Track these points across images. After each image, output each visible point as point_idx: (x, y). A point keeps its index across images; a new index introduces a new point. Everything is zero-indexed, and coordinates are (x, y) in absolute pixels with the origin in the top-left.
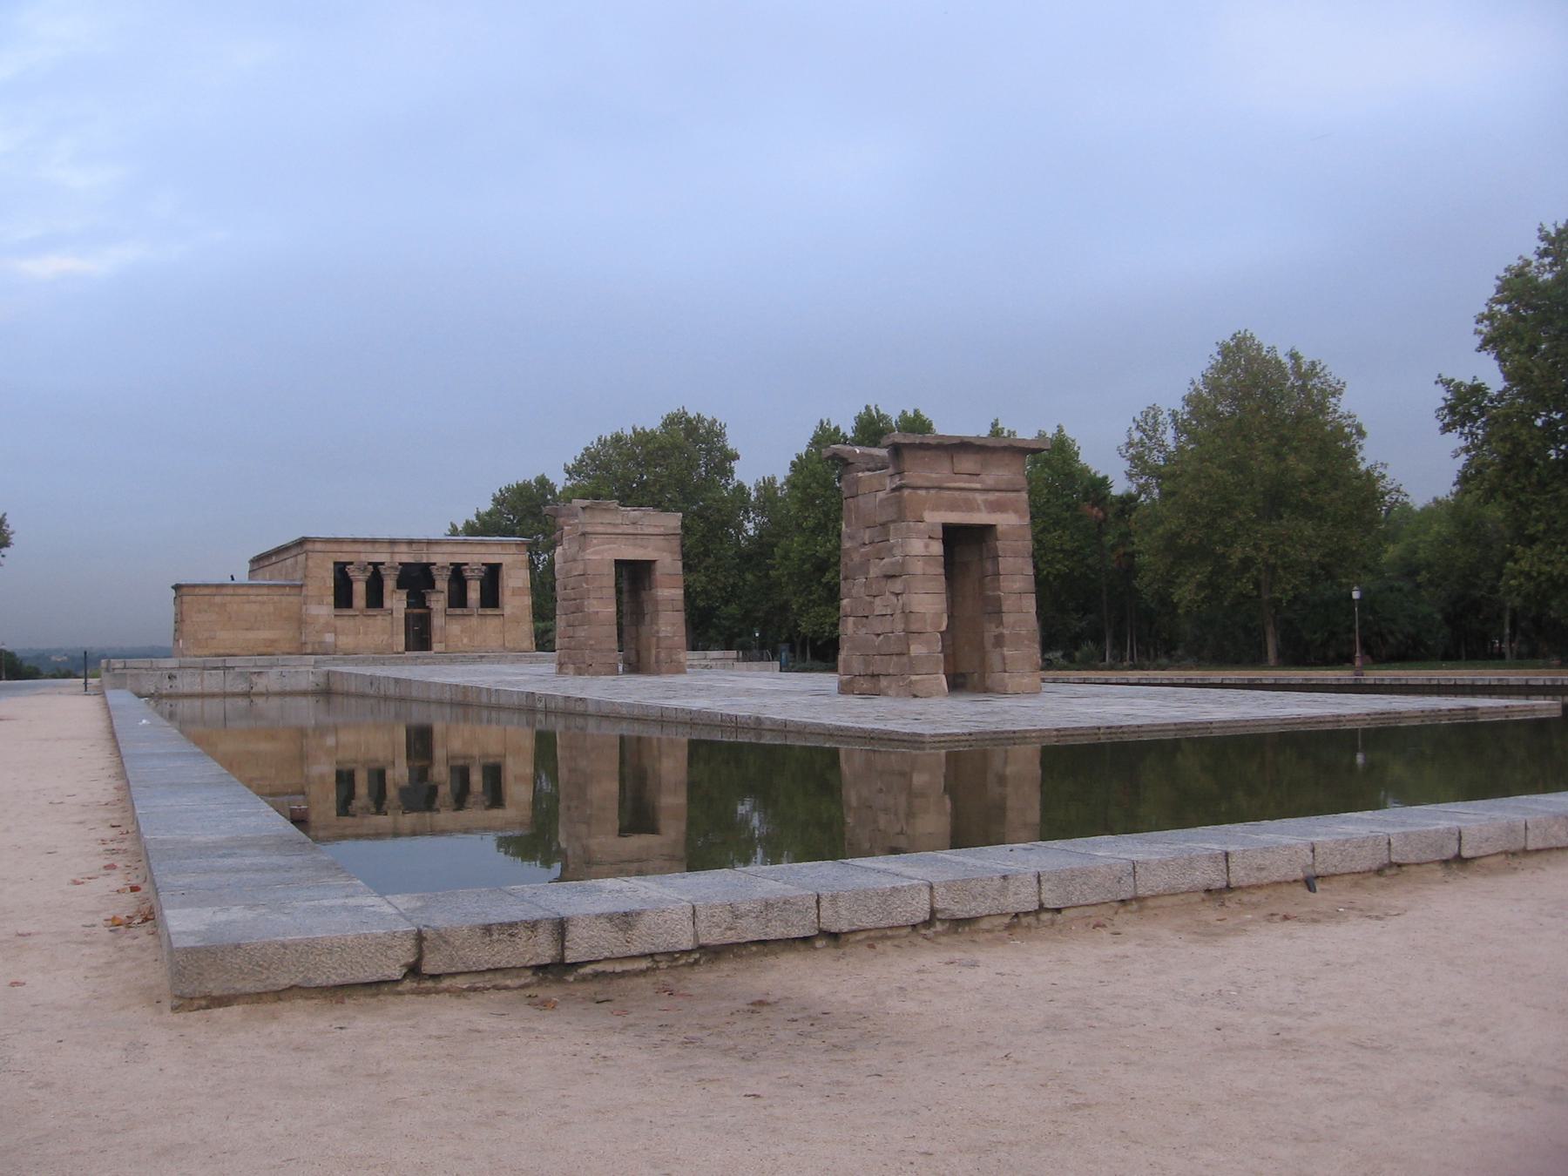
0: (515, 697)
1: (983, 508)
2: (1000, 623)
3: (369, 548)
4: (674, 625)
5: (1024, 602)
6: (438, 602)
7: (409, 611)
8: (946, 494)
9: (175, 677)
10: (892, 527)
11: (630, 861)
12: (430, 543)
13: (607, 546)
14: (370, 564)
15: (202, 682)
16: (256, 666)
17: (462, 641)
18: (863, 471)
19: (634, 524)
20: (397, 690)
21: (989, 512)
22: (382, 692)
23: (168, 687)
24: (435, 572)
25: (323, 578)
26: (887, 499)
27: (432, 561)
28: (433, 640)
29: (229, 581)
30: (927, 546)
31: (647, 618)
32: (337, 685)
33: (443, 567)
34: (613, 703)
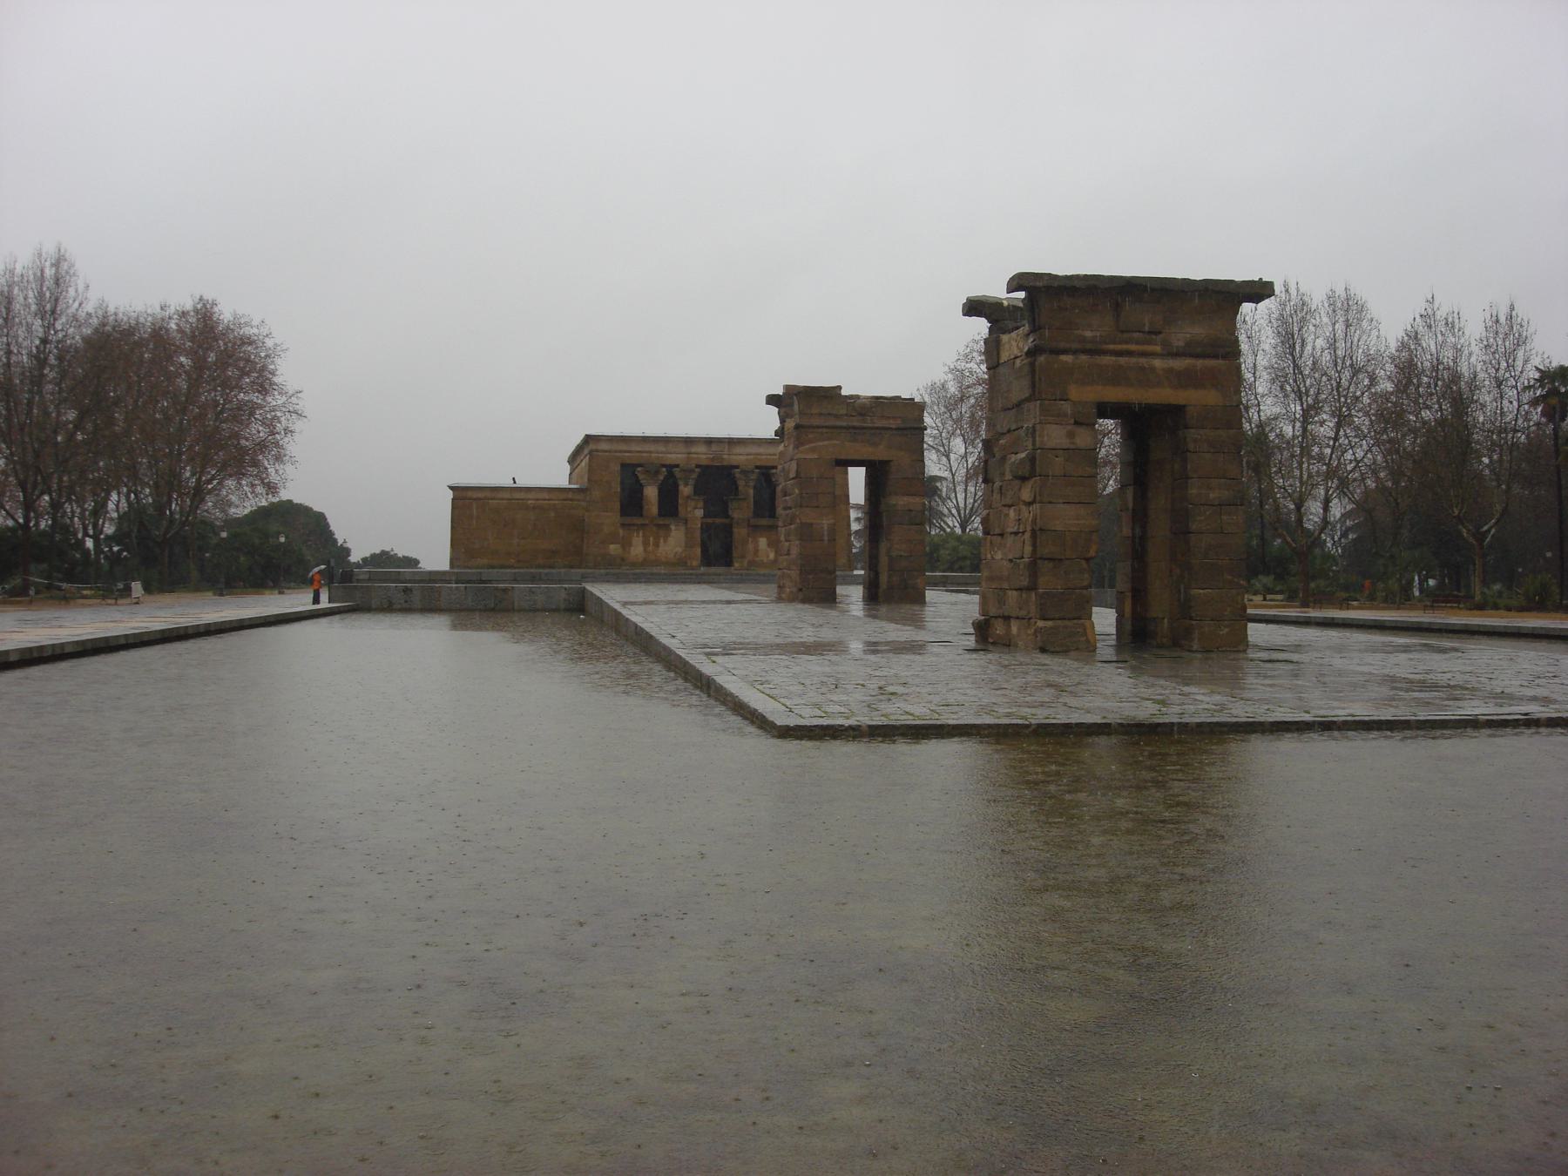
3: (661, 448)
6: (740, 512)
7: (710, 520)
8: (1107, 360)
9: (411, 590)
10: (1026, 406)
12: (732, 442)
14: (664, 466)
17: (768, 556)
19: (861, 414)
23: (402, 601)
24: (737, 475)
28: (735, 555)
29: (509, 483)
30: (1071, 435)
33: (744, 472)
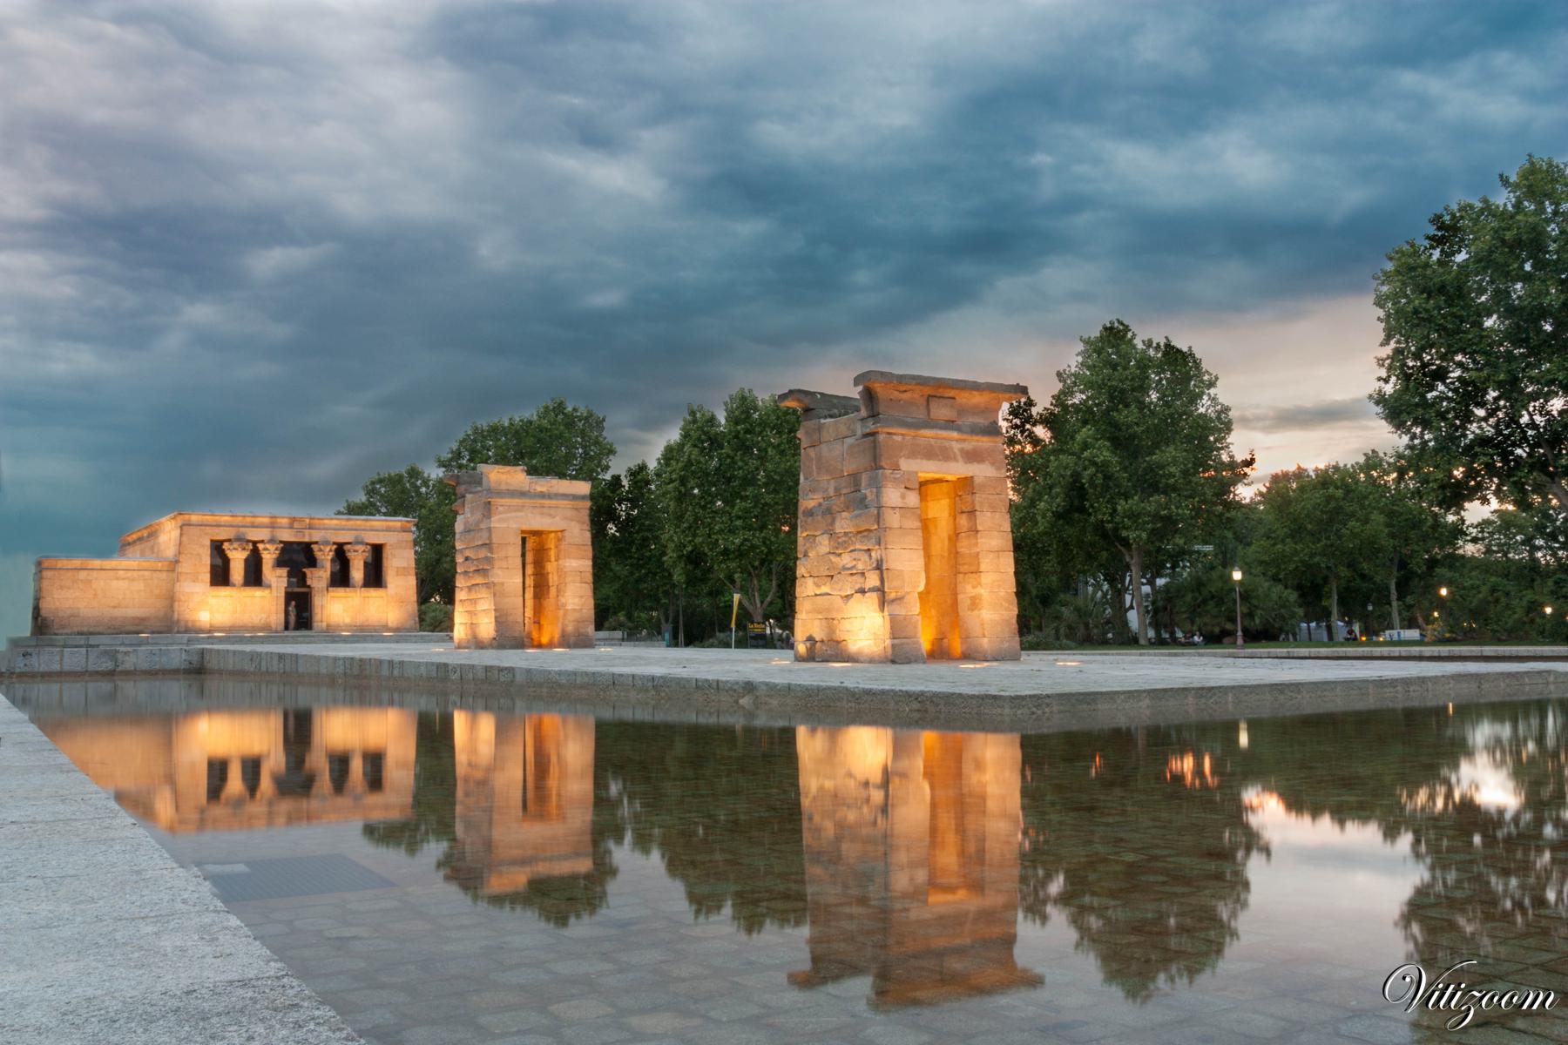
0: (423, 668)
1: (959, 457)
2: (980, 584)
4: (581, 597)
5: (1002, 560)
7: (290, 590)
11: (1525, 1032)
13: (513, 514)
15: (61, 660)
16: (122, 644)
18: (825, 417)
20: (281, 665)
21: (966, 463)
22: (264, 668)
23: (22, 665)
25: (198, 555)
26: (858, 445)
27: (314, 540)
30: (903, 497)
31: (553, 591)
32: (212, 663)
34: (549, 672)
